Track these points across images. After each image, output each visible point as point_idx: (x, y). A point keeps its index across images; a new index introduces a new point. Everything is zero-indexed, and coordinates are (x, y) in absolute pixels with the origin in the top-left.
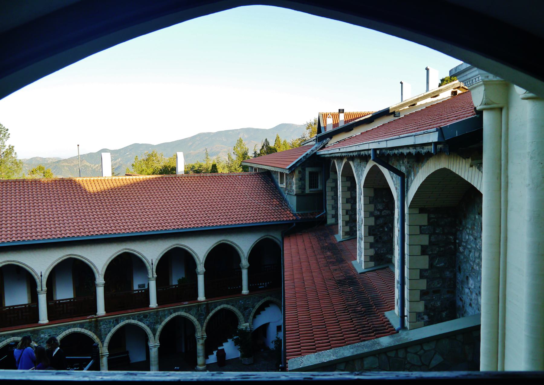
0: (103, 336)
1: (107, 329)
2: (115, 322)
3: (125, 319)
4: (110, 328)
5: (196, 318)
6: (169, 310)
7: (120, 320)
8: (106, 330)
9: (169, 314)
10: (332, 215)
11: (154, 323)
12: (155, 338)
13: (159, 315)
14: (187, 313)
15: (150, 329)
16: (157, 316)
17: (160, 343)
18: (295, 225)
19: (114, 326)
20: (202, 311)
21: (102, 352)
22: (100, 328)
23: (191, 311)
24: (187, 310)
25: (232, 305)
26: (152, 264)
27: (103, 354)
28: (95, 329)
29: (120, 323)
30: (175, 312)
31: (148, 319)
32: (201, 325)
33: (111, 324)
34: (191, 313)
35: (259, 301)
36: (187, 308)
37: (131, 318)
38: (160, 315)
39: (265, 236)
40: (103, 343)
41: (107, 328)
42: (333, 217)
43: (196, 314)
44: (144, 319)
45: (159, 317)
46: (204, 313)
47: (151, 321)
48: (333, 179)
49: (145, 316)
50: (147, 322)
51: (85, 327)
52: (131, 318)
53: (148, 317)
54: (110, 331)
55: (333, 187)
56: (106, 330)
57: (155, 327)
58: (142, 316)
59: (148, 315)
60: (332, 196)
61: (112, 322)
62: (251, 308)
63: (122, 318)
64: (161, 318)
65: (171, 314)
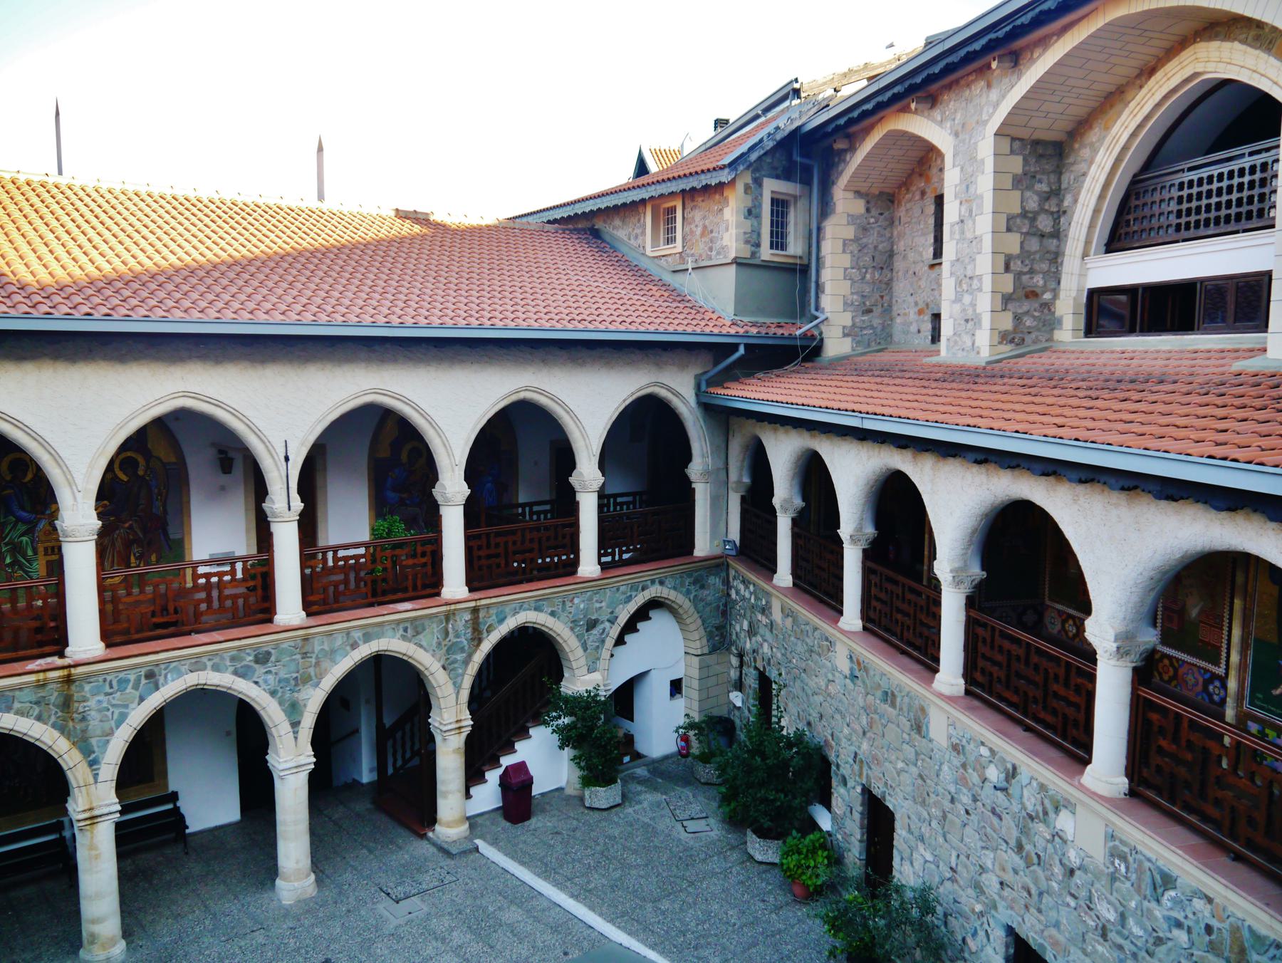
0: (94, 741)
1: (111, 710)
2: (143, 681)
3: (183, 669)
4: (126, 706)
5: (439, 661)
6: (348, 632)
7: (163, 672)
8: (106, 716)
9: (348, 648)
10: (844, 327)
11: (293, 682)
12: (296, 738)
13: (313, 652)
14: (410, 641)
15: (280, 704)
16: (305, 655)
17: (315, 756)
18: (742, 350)
19: (142, 699)
20: (457, 636)
21: (94, 805)
22: (81, 710)
23: (420, 636)
24: (409, 630)
25: (553, 614)
26: (287, 459)
27: (96, 813)
28: (60, 714)
29: (163, 685)
30: (367, 638)
31: (273, 669)
32: (454, 683)
33: (129, 690)
34: (424, 644)
35: (629, 599)
36: (408, 625)
37: (209, 664)
38: (316, 651)
39: (648, 386)
40: (95, 767)
41: (113, 706)
42: (845, 335)
43: (439, 644)
44: (256, 666)
45: (313, 660)
46: (465, 643)
47: (283, 674)
48: (848, 215)
49: (262, 658)
50: (270, 677)
51: (17, 705)
52: (209, 664)
53: (273, 659)
54: (123, 717)
55: (851, 240)
56: (109, 714)
57: (296, 695)
58: (251, 658)
59: (273, 651)
60: (846, 269)
61: (131, 684)
62: (607, 624)
63: (173, 665)
64: (317, 664)
65: (354, 646)
